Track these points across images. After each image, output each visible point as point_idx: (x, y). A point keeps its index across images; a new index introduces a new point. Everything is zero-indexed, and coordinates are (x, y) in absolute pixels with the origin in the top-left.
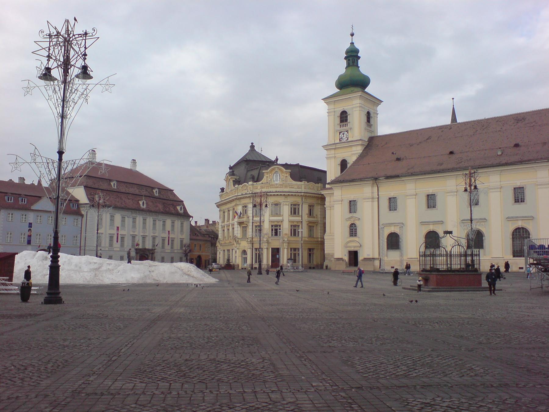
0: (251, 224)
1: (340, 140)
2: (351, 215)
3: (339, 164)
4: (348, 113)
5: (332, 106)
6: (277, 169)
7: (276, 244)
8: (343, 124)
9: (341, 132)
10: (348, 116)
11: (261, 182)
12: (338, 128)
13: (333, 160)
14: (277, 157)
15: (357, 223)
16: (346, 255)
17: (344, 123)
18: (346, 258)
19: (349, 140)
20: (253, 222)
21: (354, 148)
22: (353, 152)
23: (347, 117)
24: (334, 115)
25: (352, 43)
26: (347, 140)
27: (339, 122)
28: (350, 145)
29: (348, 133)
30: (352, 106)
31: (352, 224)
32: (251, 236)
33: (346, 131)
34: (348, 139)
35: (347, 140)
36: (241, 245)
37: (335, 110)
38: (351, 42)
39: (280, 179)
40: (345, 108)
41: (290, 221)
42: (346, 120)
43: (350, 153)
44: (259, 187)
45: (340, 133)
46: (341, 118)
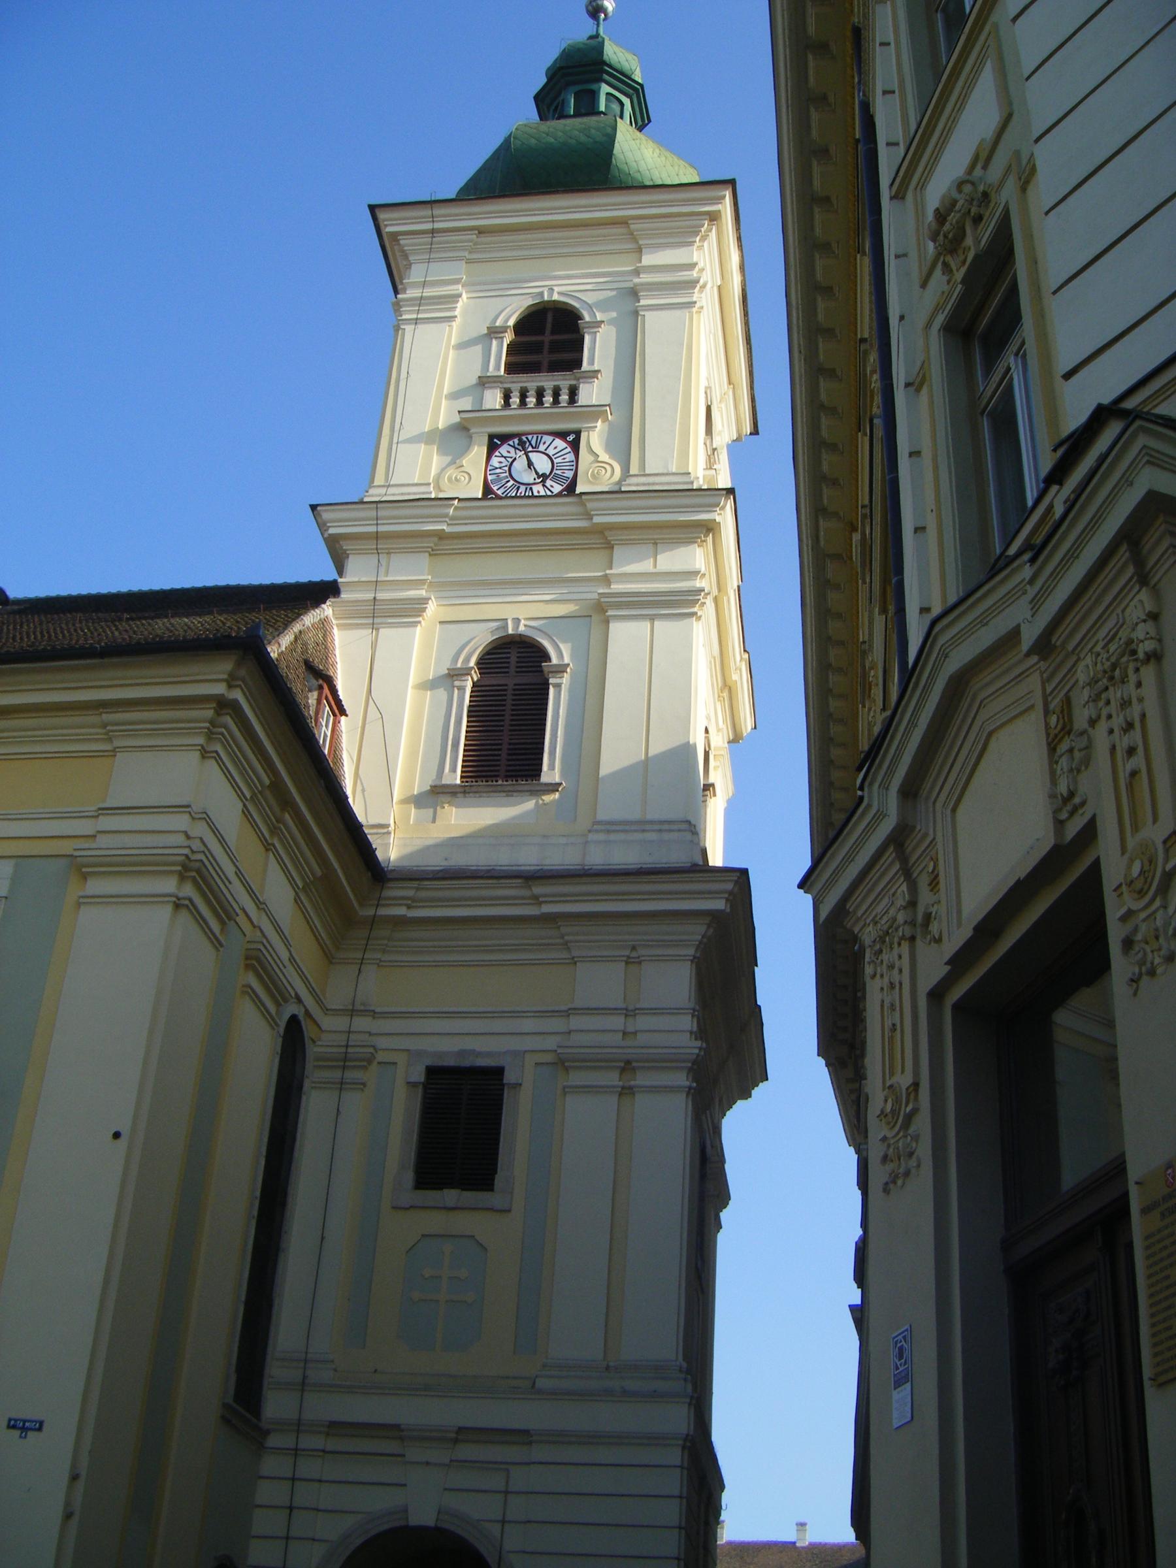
8: (532, 382)
9: (505, 438)
17: (548, 381)
29: (575, 446)
33: (562, 435)
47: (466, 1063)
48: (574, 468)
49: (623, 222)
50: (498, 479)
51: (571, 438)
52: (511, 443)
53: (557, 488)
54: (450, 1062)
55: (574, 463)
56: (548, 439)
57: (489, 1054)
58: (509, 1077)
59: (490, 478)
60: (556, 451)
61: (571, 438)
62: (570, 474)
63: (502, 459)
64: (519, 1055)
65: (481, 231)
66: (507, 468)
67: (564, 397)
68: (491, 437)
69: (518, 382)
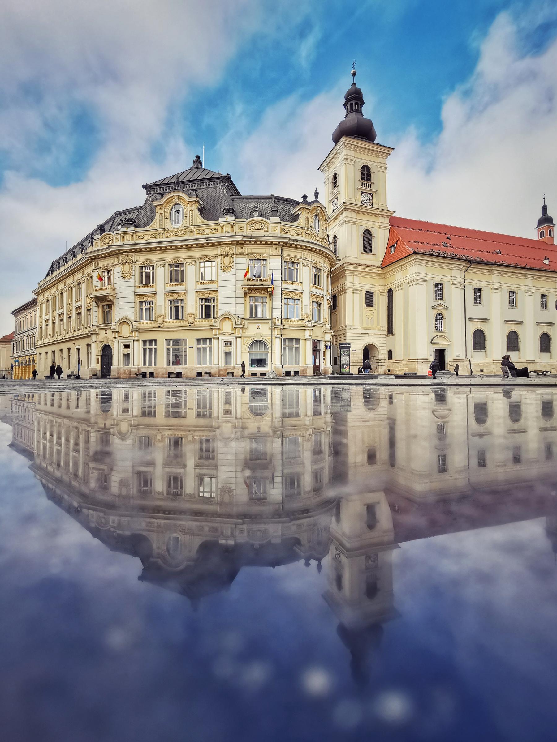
0: (279, 294)
1: (362, 203)
2: (437, 302)
3: (362, 235)
4: (372, 170)
5: (351, 153)
6: (319, 209)
7: (318, 334)
8: (365, 182)
9: (363, 193)
10: (372, 176)
11: (295, 224)
12: (359, 185)
13: (354, 227)
14: (316, 190)
15: (444, 313)
16: (432, 355)
18: (432, 359)
19: (374, 206)
20: (282, 291)
21: (381, 219)
22: (381, 224)
23: (370, 175)
25: (354, 84)
27: (361, 179)
28: (379, 213)
29: (372, 196)
30: (378, 165)
31: (439, 314)
32: (280, 316)
33: (370, 194)
34: (372, 204)
35: (371, 206)
36: (247, 331)
37: (356, 159)
38: (353, 82)
39: (319, 229)
40: (369, 162)
41: (328, 300)
42: (369, 180)
43: (378, 224)
44: (292, 232)
45: (362, 193)
46: (362, 174)
49: (377, 151)
53: (371, 204)
56: (368, 194)
58: (374, 293)
65: (358, 146)
67: (370, 186)
68: (361, 192)
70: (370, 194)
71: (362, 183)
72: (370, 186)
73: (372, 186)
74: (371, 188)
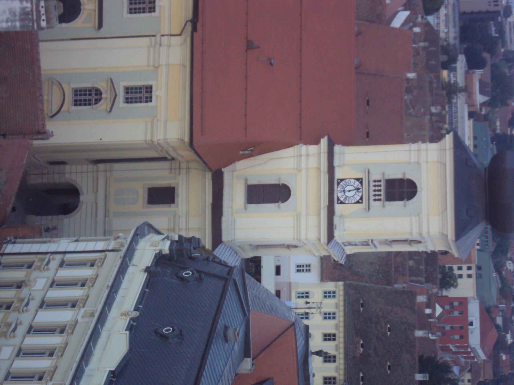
1: (342, 180)
9: (361, 183)
24: (409, 163)
26: (338, 199)
27: (387, 177)
29: (358, 202)
33: (361, 198)
34: (342, 203)
42: (391, 197)
45: (360, 180)
47: (176, 195)
48: (349, 203)
50: (346, 183)
51: (360, 201)
52: (360, 184)
53: (342, 199)
54: (176, 192)
55: (351, 203)
57: (178, 200)
58: (172, 205)
59: (347, 180)
60: (356, 197)
61: (360, 201)
62: (347, 202)
63: (353, 183)
64: (177, 206)
66: (350, 184)
67: (377, 198)
68: (362, 179)
69: (382, 183)
70: (361, 198)
71: (380, 181)
72: (377, 198)
73: (378, 203)
74: (375, 200)
